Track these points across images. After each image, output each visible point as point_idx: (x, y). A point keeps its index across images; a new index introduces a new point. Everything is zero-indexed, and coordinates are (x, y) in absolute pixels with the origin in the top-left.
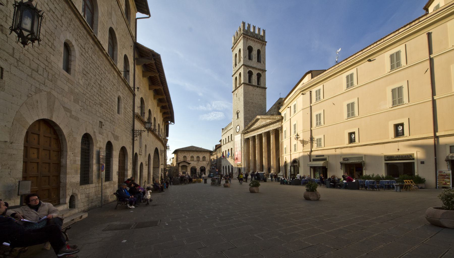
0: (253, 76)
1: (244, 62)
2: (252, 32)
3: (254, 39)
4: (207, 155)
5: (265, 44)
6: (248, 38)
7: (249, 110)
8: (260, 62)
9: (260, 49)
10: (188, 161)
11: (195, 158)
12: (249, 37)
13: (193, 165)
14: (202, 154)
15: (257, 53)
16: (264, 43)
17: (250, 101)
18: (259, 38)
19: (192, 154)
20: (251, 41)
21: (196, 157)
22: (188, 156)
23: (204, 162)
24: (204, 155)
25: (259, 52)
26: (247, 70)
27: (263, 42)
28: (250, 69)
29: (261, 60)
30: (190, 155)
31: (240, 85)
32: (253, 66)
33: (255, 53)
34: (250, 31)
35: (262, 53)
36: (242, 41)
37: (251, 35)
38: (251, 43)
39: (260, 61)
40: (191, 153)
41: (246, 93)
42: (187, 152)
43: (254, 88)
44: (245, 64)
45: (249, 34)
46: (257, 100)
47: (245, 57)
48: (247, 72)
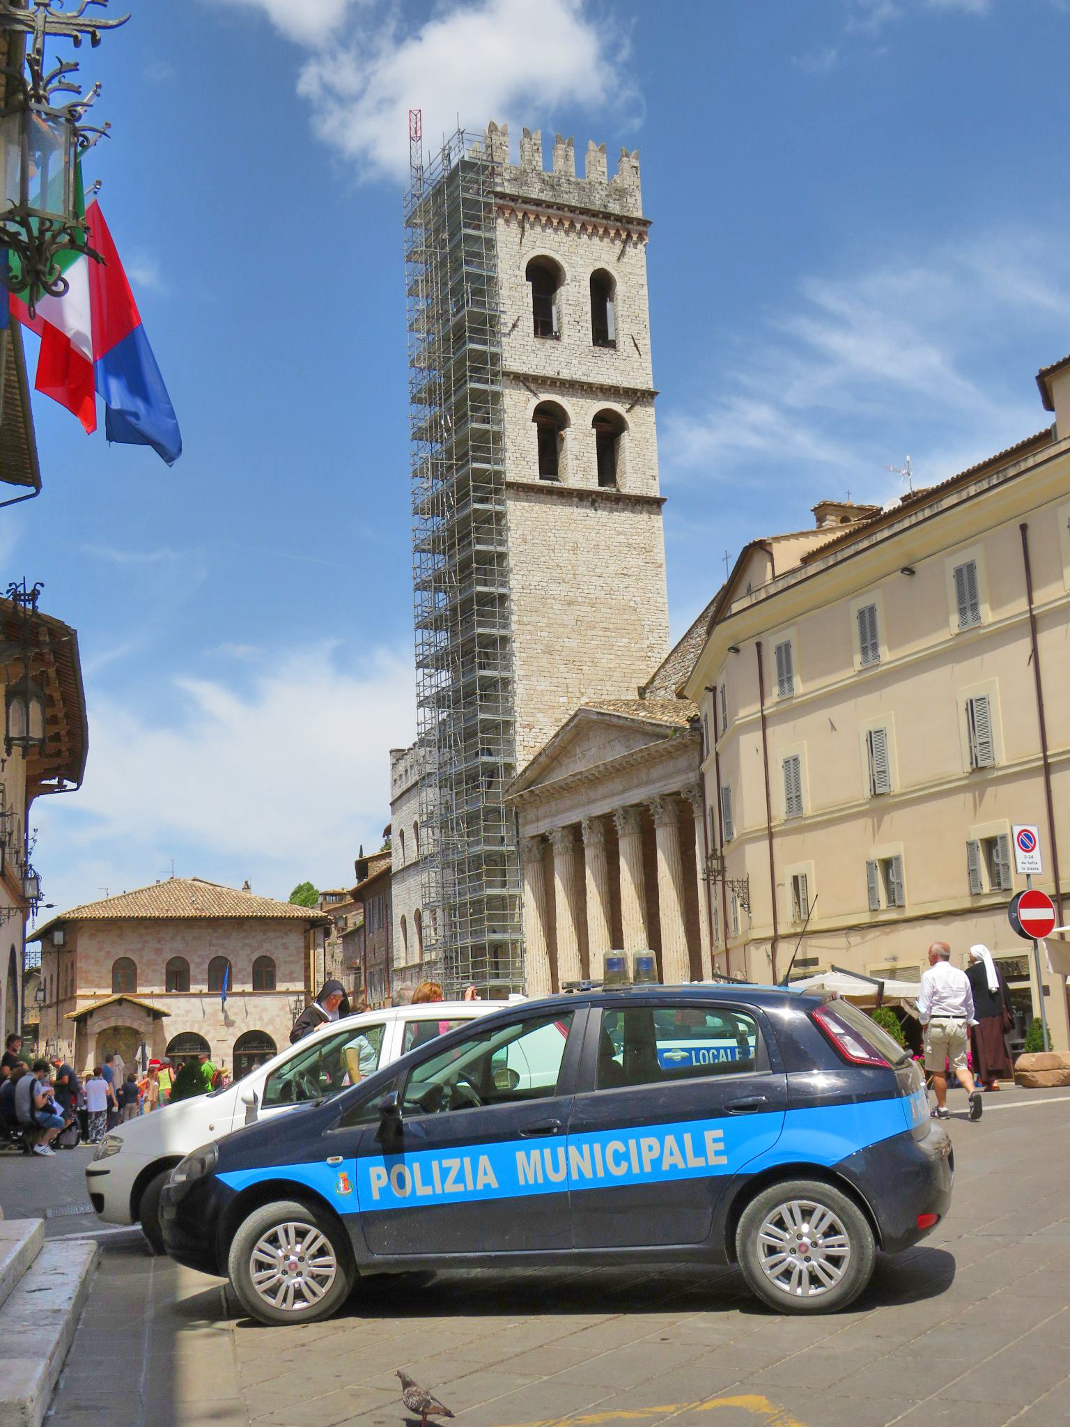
0: (569, 434)
3: (568, 214)
4: (285, 947)
7: (549, 651)
8: (612, 345)
12: (534, 208)
13: (185, 1023)
14: (247, 941)
17: (555, 590)
21: (206, 966)
28: (545, 397)
30: (158, 952)
32: (565, 375)
39: (611, 337)
41: (525, 541)
42: (143, 931)
46: (600, 582)
48: (530, 413)
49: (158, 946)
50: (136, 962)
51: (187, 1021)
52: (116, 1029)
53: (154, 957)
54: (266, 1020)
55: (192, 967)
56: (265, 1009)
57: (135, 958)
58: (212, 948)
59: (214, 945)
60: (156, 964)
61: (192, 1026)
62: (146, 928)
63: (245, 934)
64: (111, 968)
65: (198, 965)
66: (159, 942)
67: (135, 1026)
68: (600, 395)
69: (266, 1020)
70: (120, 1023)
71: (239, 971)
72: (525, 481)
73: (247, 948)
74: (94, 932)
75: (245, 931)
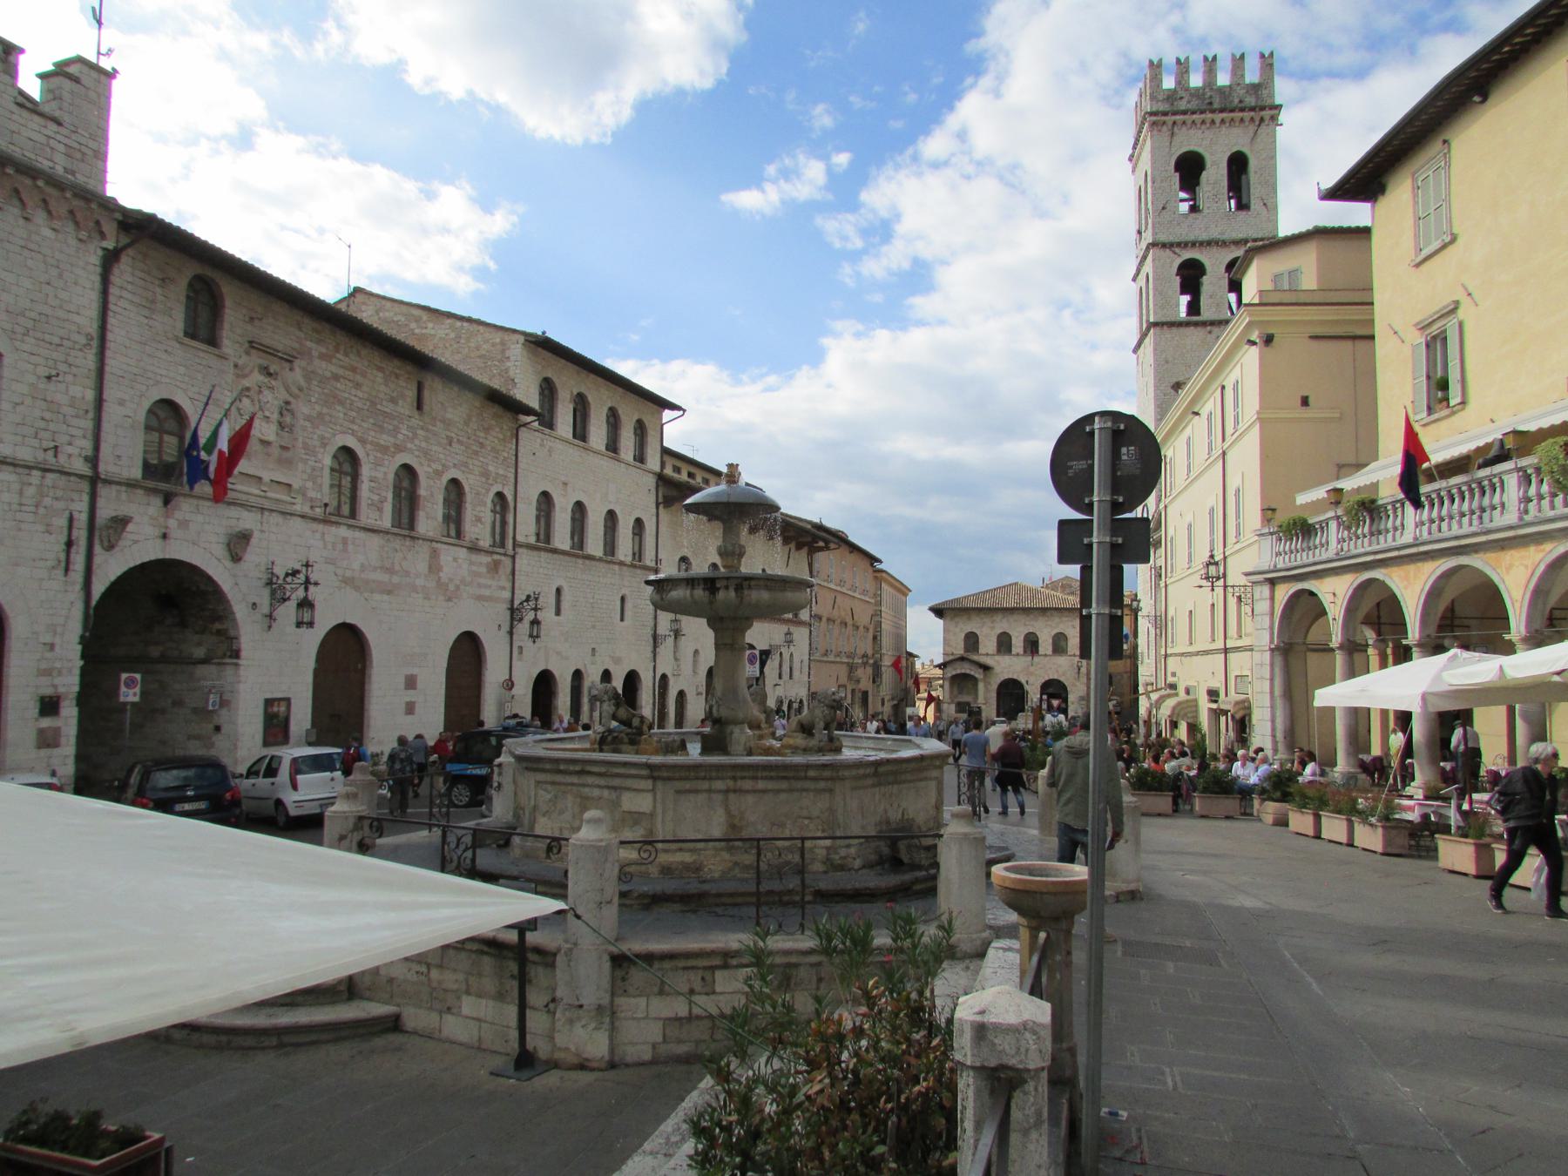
1: (1154, 234)
2: (1197, 89)
5: (1274, 118)
6: (1174, 123)
9: (1246, 150)
10: (987, 654)
11: (1018, 644)
14: (1049, 623)
15: (1225, 172)
16: (1267, 114)
18: (1236, 101)
20: (1192, 132)
23: (1062, 661)
24: (1062, 626)
25: (1238, 164)
26: (1172, 262)
27: (1256, 115)
28: (1188, 255)
29: (1252, 197)
31: (1148, 329)
32: (1204, 237)
33: (1215, 175)
34: (1187, 89)
35: (1253, 164)
36: (1148, 143)
37: (1194, 105)
38: (1190, 140)
40: (998, 617)
41: (1167, 362)
43: (1210, 332)
44: (1163, 238)
45: (1183, 105)
47: (1164, 208)
48: (1175, 270)
67: (972, 673)
68: (1233, 247)
72: (1168, 319)
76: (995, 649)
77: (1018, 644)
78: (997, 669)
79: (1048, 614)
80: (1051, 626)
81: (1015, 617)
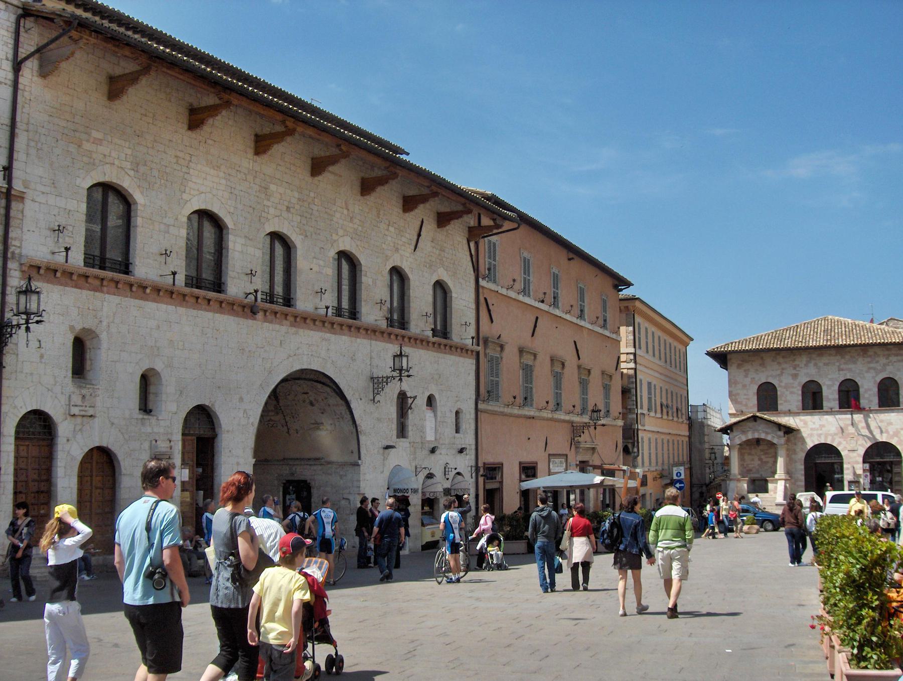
11: (830, 395)
13: (819, 435)
14: (872, 365)
19: (806, 365)
22: (786, 379)
30: (795, 376)
42: (781, 360)
49: (794, 372)
50: (777, 386)
51: (821, 434)
52: (758, 441)
53: (792, 381)
54: (891, 433)
55: (824, 389)
56: (890, 424)
57: (775, 382)
58: (841, 372)
59: (842, 370)
60: (793, 387)
61: (826, 437)
62: (783, 357)
63: (869, 359)
64: (755, 391)
65: (829, 387)
66: (795, 368)
69: (891, 433)
70: (763, 436)
71: (866, 391)
73: (872, 371)
74: (741, 362)
75: (870, 356)
76: (800, 404)
77: (830, 395)
78: (805, 433)
79: (871, 352)
80: (874, 369)
81: (825, 359)
